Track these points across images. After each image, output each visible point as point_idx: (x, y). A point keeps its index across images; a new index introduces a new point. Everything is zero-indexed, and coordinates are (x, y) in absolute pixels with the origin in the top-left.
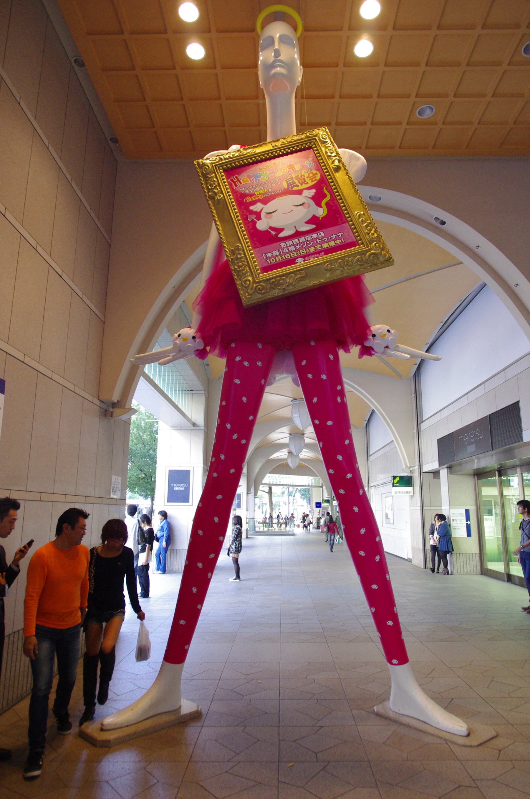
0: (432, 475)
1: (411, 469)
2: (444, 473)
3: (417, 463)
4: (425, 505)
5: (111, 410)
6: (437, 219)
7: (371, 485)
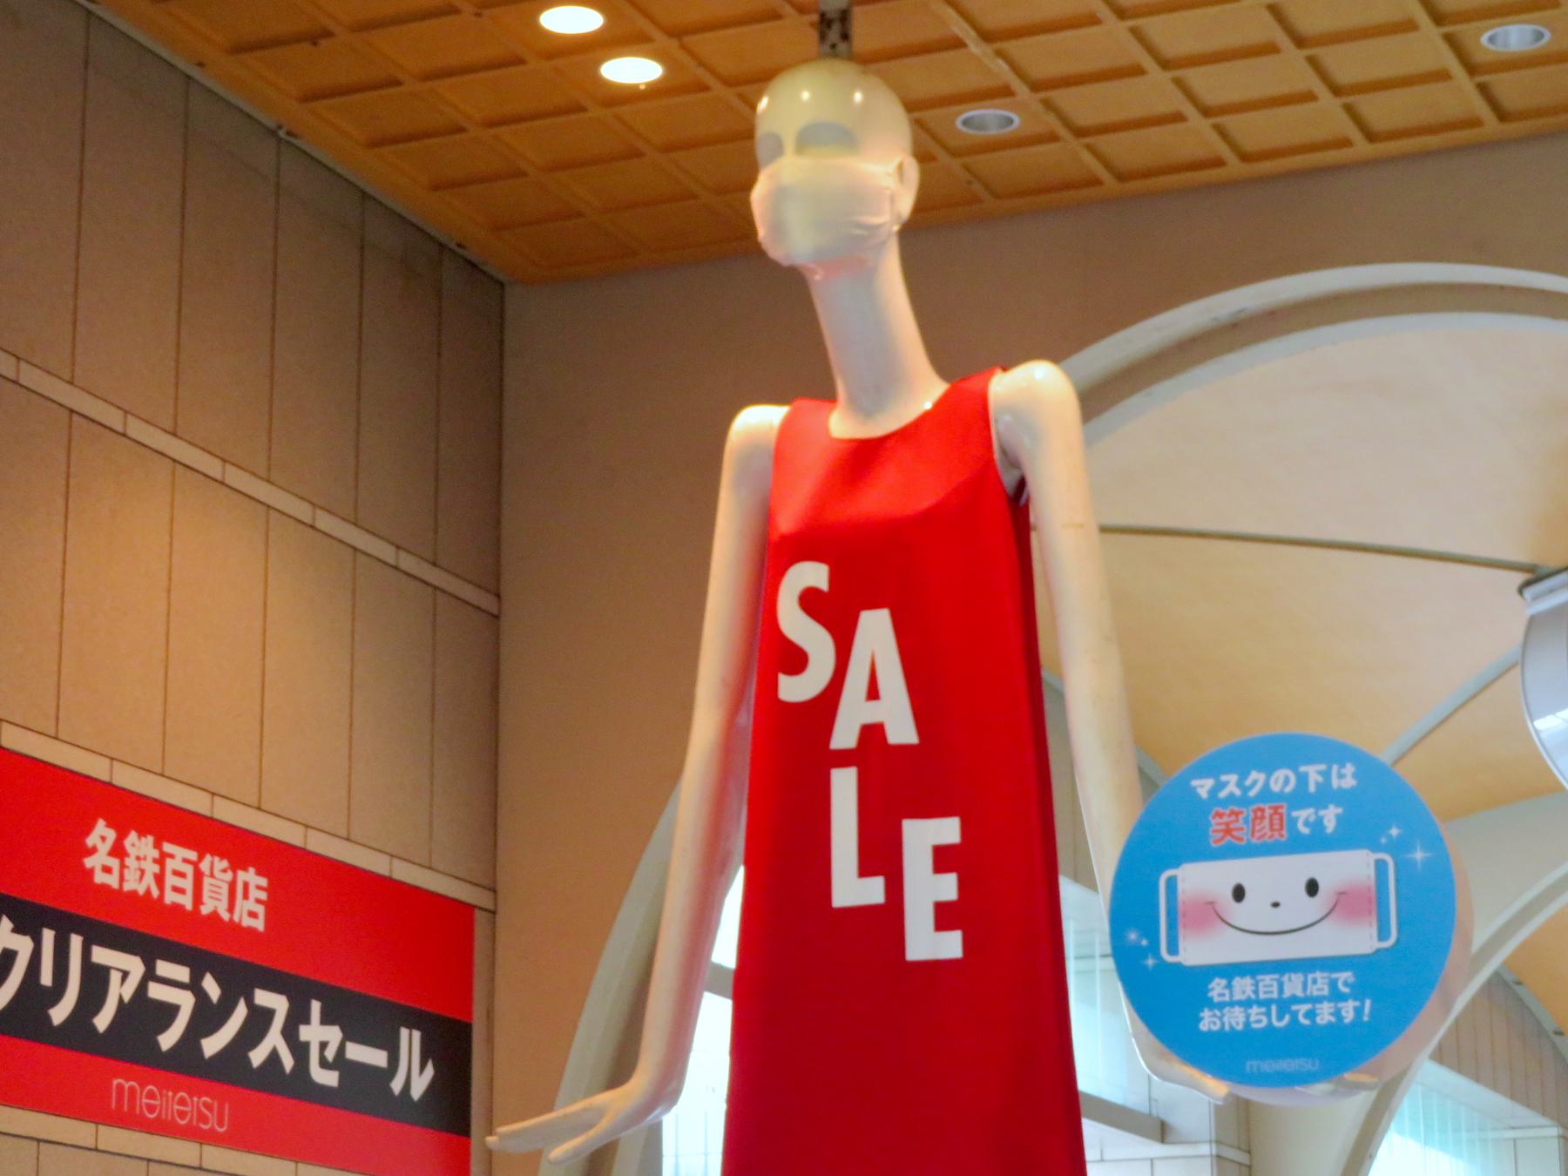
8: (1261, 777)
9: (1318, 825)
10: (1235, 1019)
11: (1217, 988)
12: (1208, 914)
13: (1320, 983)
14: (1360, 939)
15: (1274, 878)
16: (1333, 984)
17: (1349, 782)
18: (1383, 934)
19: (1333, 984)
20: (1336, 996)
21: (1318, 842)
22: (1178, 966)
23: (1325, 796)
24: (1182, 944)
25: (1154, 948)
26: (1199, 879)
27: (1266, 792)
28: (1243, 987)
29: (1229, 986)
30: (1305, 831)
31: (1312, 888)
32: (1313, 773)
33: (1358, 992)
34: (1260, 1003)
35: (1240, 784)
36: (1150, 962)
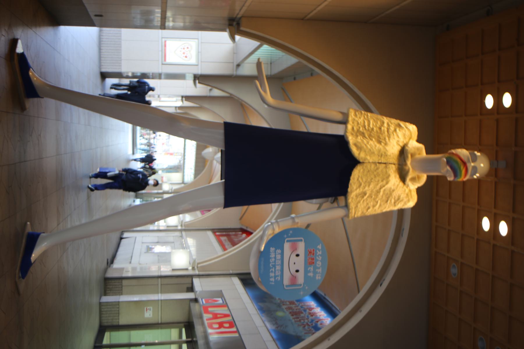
0: (190, 286)
1: (196, 267)
2: (191, 295)
3: (201, 273)
4: (163, 279)
5: (235, 23)
6: (384, 280)
7: (184, 233)
8: (320, 259)
9: (310, 272)
10: (272, 255)
11: (279, 251)
12: (294, 248)
13: (278, 273)
14: (286, 281)
15: (300, 263)
16: (278, 276)
17: (317, 278)
18: (287, 286)
19: (278, 276)
20: (275, 277)
21: (306, 272)
22: (284, 242)
23: (315, 273)
24: (288, 243)
25: (288, 237)
26: (301, 247)
27: (317, 260)
28: (279, 257)
29: (279, 254)
30: (309, 269)
31: (297, 271)
32: (320, 270)
33: (276, 281)
34: (275, 261)
35: (319, 255)
36: (285, 236)
